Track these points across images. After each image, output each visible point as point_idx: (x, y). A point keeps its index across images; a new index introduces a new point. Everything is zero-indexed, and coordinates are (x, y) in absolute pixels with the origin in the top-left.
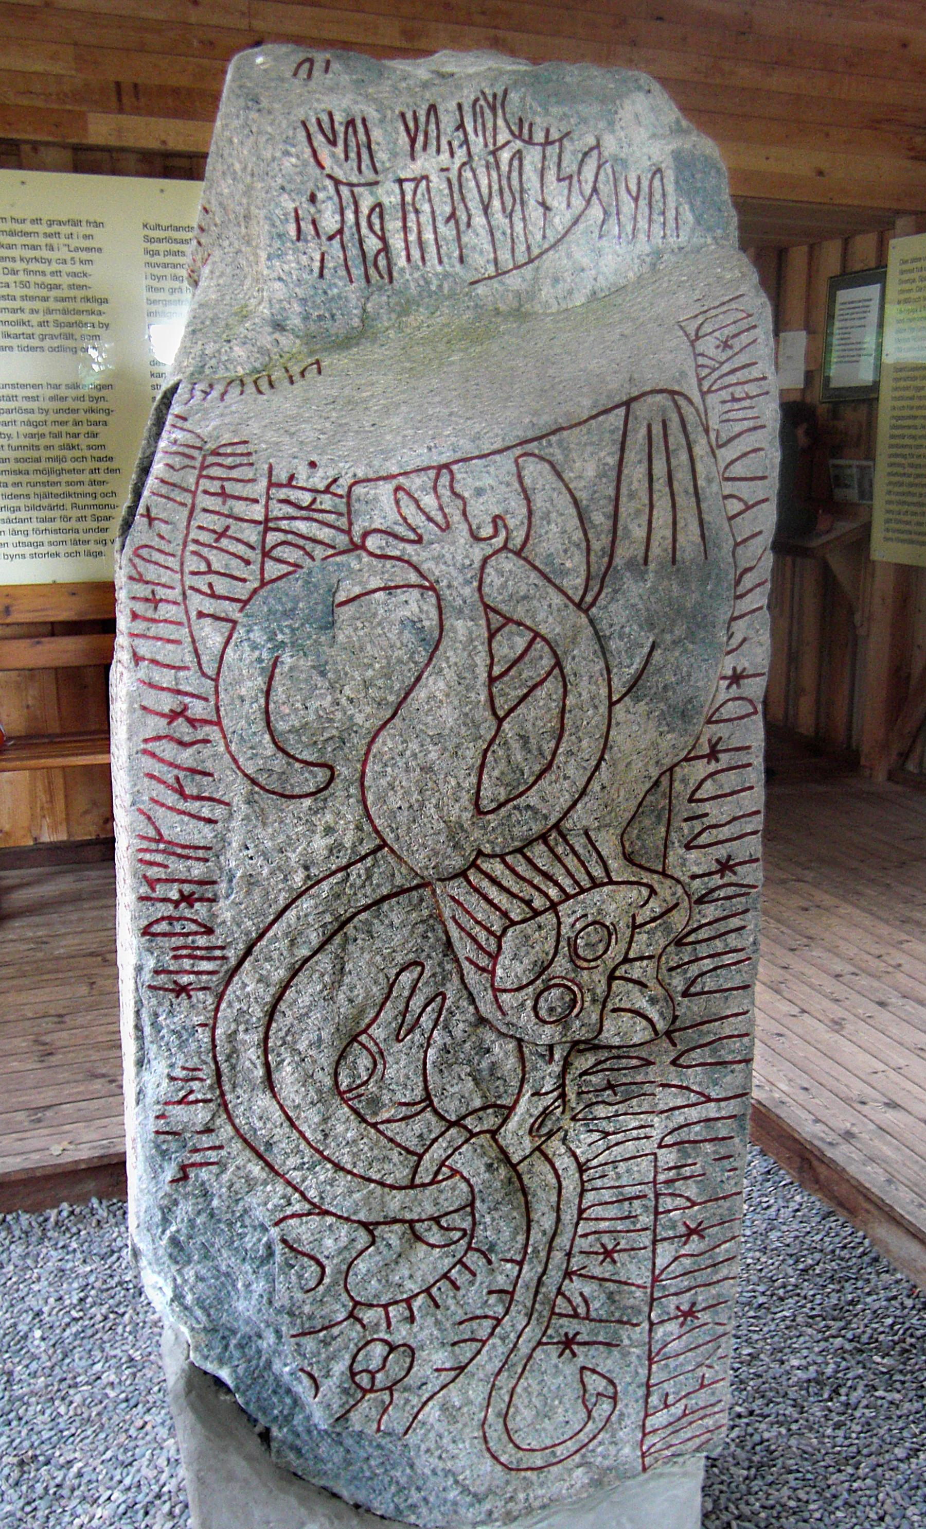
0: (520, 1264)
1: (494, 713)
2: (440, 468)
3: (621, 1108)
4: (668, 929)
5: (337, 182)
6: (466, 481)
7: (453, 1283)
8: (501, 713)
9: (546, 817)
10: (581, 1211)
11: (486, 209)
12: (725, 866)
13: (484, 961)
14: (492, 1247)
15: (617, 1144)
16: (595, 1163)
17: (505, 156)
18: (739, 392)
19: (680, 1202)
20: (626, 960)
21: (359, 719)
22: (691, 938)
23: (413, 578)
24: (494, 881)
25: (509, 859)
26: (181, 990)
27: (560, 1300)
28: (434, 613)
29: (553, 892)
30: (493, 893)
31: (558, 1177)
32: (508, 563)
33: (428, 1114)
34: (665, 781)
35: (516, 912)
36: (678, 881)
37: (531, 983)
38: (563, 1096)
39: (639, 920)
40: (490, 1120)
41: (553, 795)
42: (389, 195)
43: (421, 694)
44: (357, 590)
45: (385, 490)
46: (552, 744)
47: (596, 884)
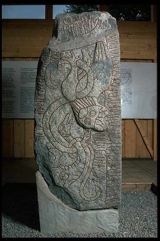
0: (85, 164)
1: (78, 79)
2: (71, 50)
3: (100, 142)
4: (105, 114)
5: (66, 25)
6: (74, 52)
7: (75, 165)
8: (79, 80)
9: (85, 94)
10: (94, 158)
11: (84, 27)
12: (114, 107)
13: (77, 114)
14: (80, 160)
15: (100, 148)
16: (96, 150)
17: (86, 21)
18: (113, 43)
19: (110, 160)
20: (98, 117)
21: (61, 79)
22: (109, 117)
23: (68, 62)
24: (79, 103)
25: (80, 100)
26: (39, 114)
27: (91, 172)
28: (70, 67)
29: (87, 105)
30: (78, 104)
31: (90, 151)
32: (80, 61)
33: (71, 136)
34: (104, 92)
35: (82, 107)
36: (107, 107)
37: (84, 118)
38: (90, 138)
39: (100, 112)
40: (80, 140)
41: (86, 92)
42: (72, 26)
43: (69, 77)
44: (60, 64)
45: (64, 53)
46: (86, 85)
47: (93, 105)
